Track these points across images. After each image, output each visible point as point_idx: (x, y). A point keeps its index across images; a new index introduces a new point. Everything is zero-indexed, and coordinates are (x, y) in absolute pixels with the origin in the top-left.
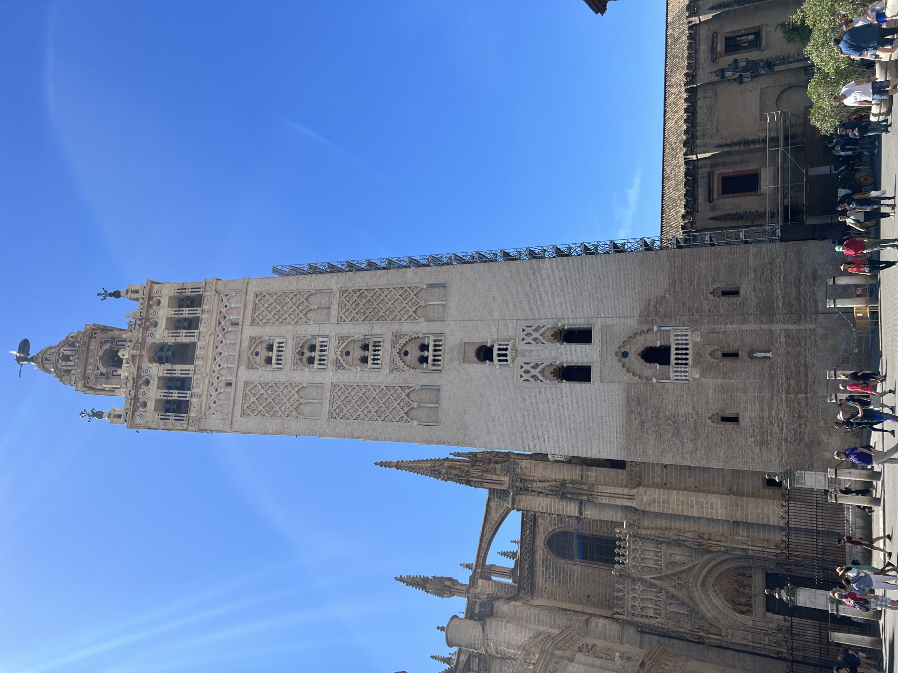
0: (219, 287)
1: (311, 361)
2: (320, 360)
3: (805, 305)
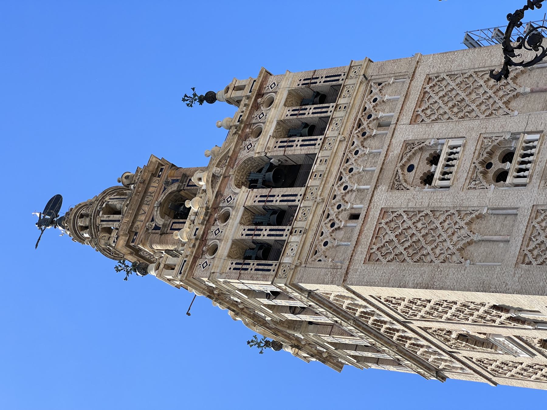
0: (370, 72)
1: (502, 176)
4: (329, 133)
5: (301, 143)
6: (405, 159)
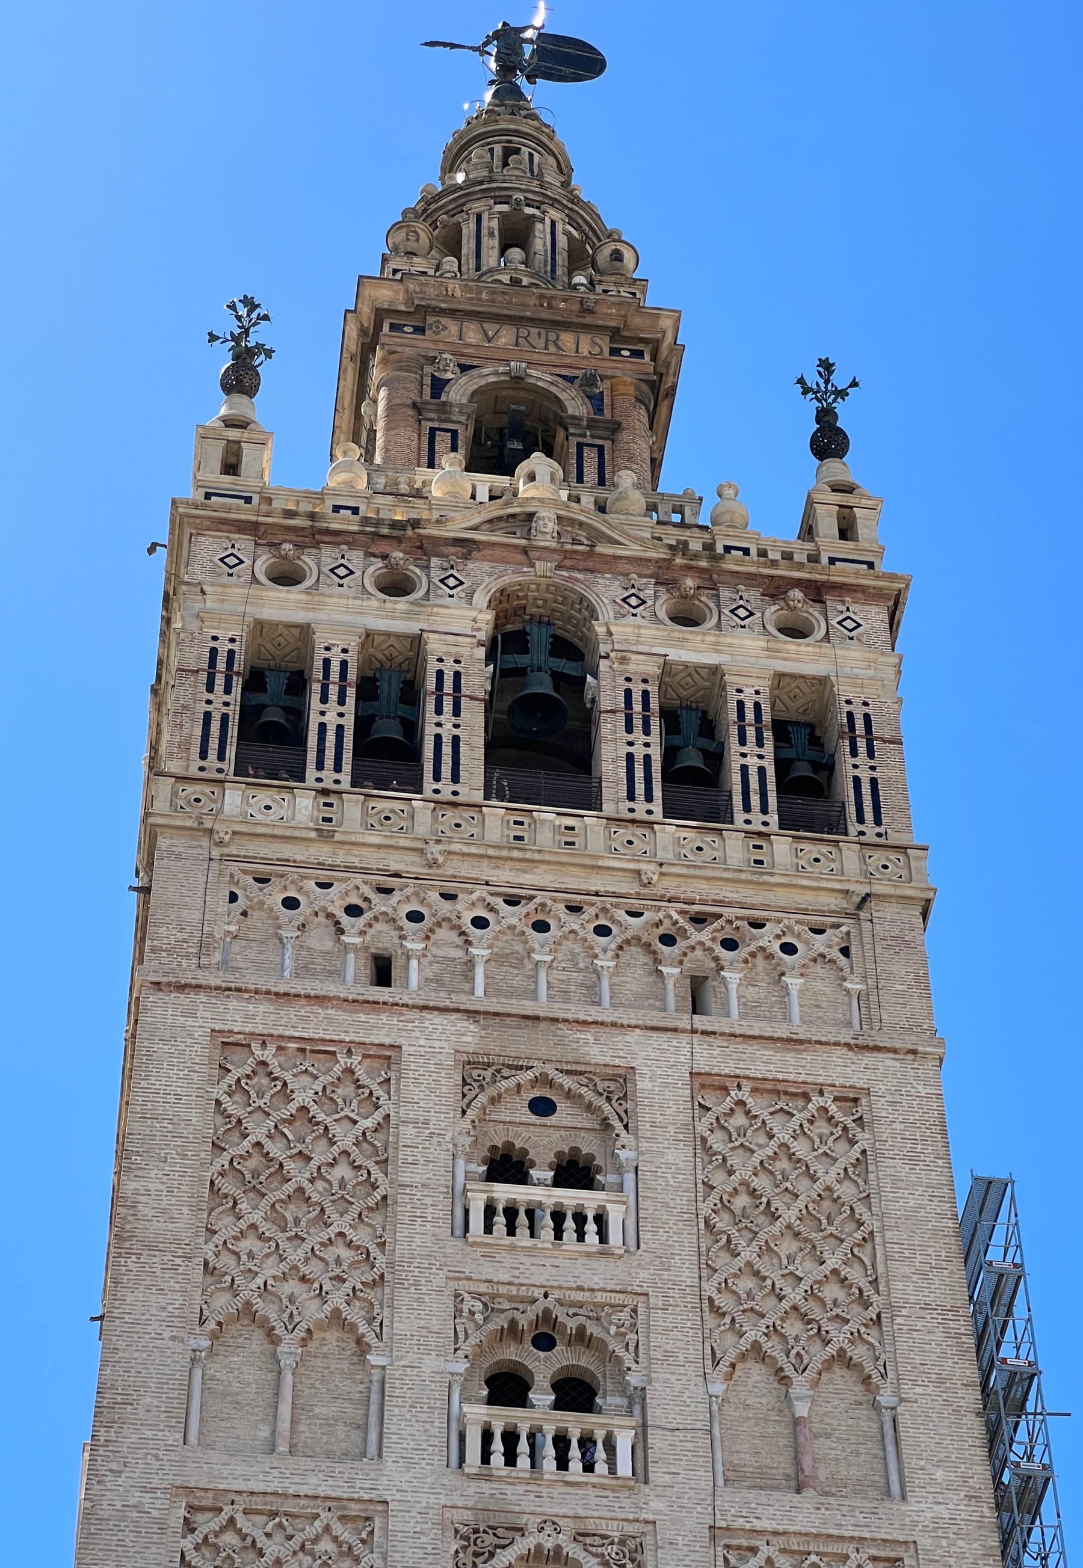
0: (885, 913)
1: (507, 1387)
2: (510, 1438)
5: (639, 751)
6: (567, 1082)
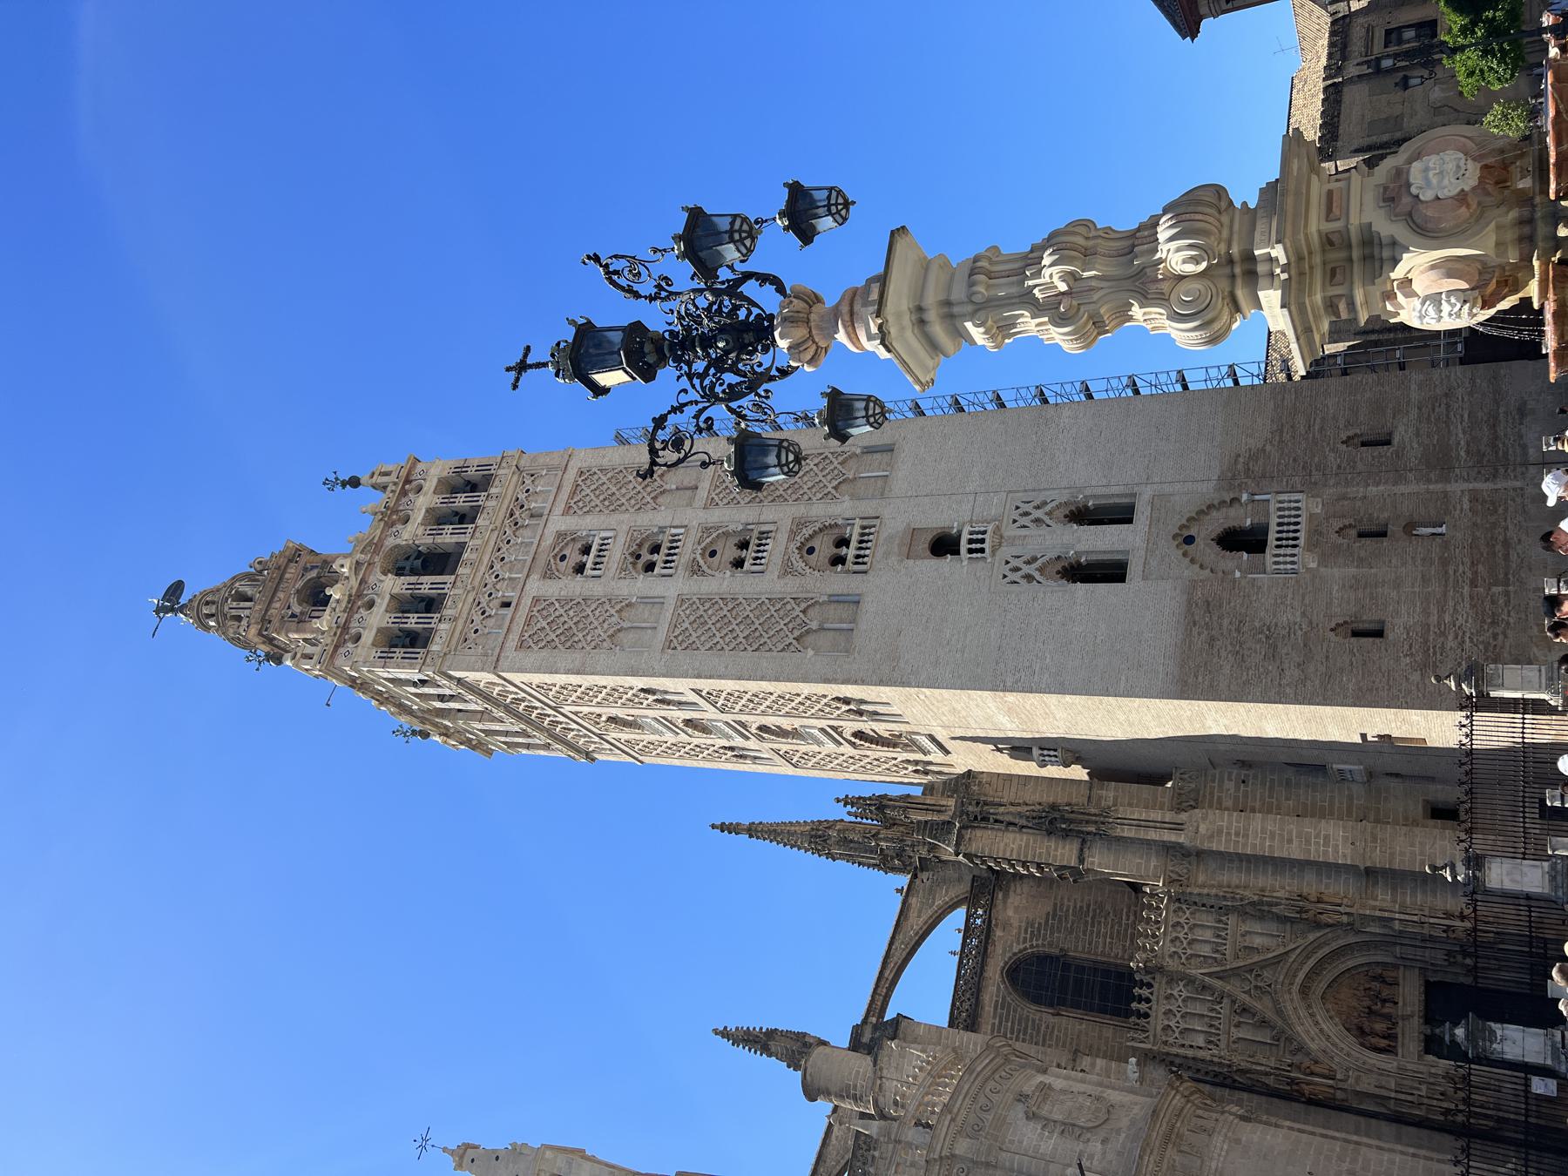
0: (522, 463)
1: (650, 567)
3: (1506, 453)
4: (480, 521)
